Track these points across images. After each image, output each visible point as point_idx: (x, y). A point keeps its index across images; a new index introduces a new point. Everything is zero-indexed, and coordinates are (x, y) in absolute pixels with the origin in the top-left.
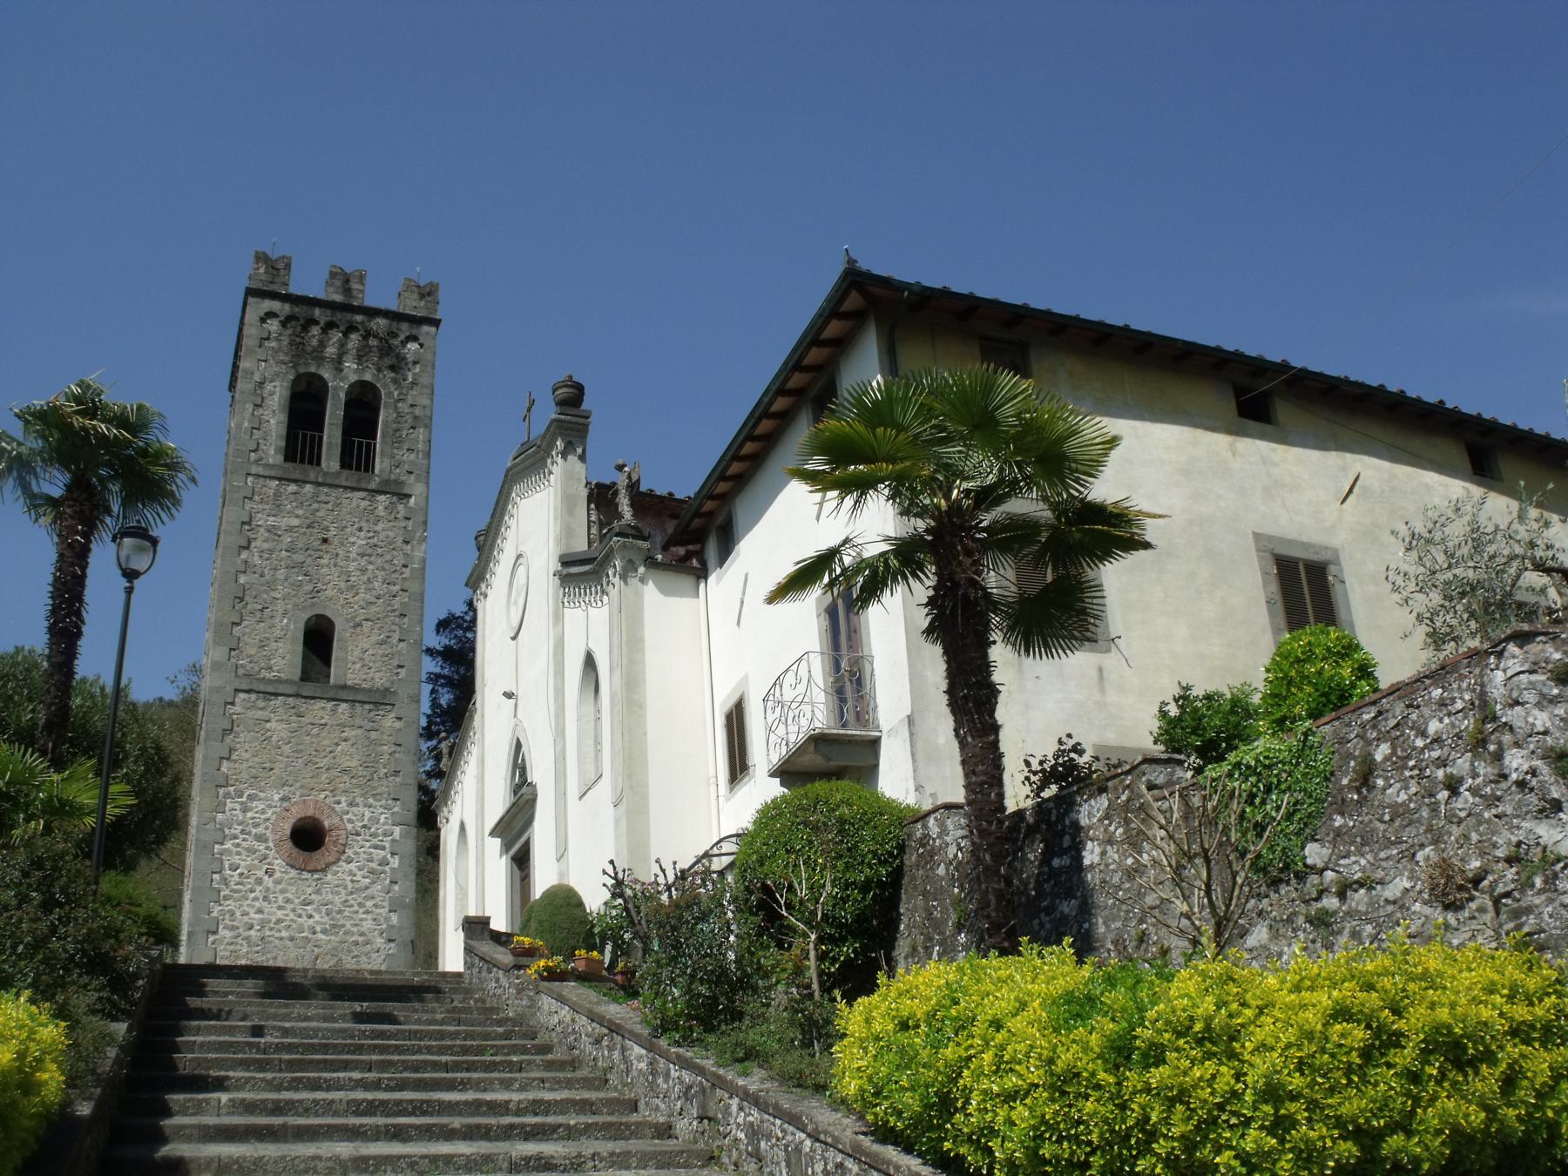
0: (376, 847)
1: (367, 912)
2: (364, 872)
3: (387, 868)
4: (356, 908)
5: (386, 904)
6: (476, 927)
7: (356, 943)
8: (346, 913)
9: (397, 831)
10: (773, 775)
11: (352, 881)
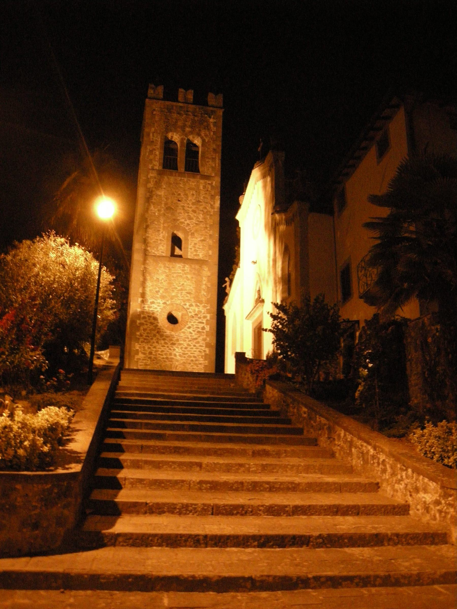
0: (200, 323)
1: (197, 348)
2: (196, 332)
3: (204, 331)
4: (192, 347)
5: (204, 345)
6: (240, 357)
7: (192, 361)
8: (189, 349)
9: (208, 316)
10: (361, 297)
11: (191, 336)
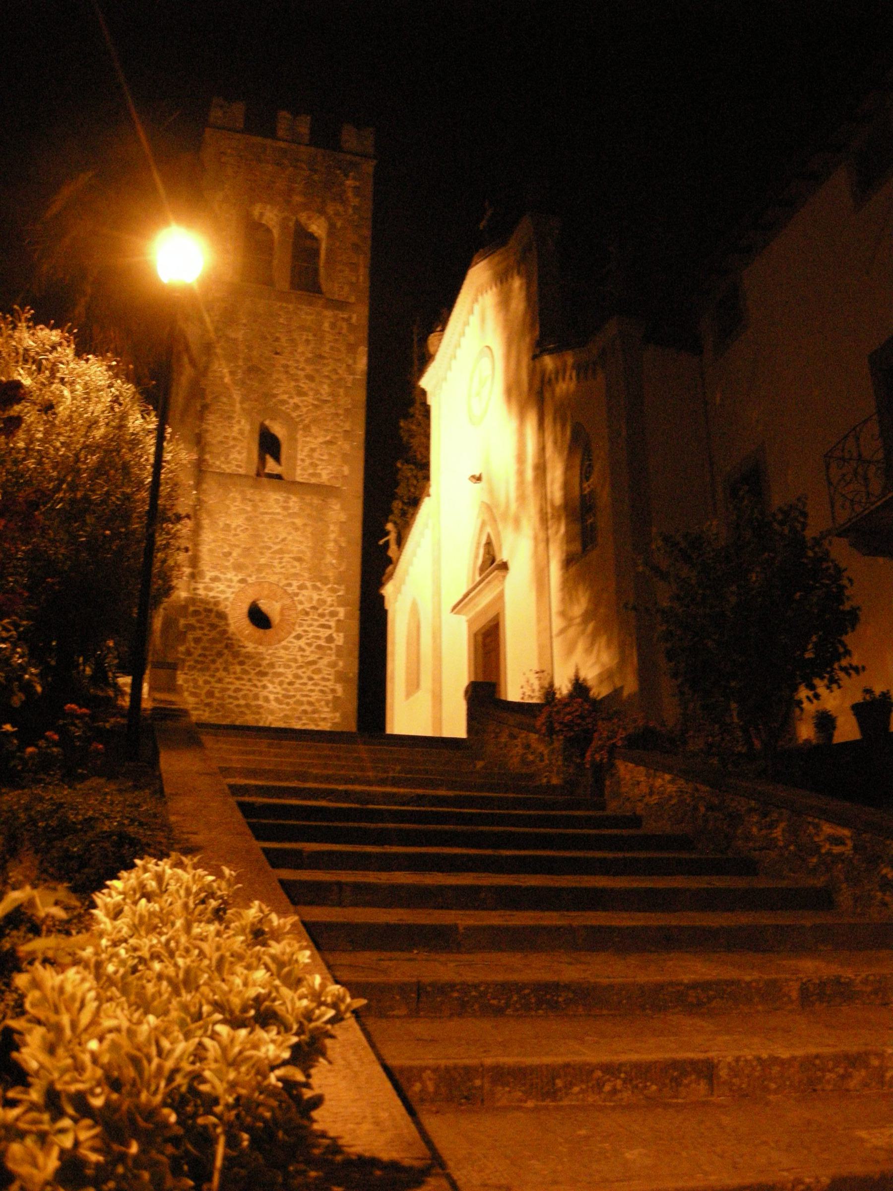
0: (323, 626)
1: (316, 684)
2: (313, 648)
3: (333, 645)
4: (305, 680)
7: (305, 712)
8: (297, 686)
9: (342, 612)
11: (302, 656)
